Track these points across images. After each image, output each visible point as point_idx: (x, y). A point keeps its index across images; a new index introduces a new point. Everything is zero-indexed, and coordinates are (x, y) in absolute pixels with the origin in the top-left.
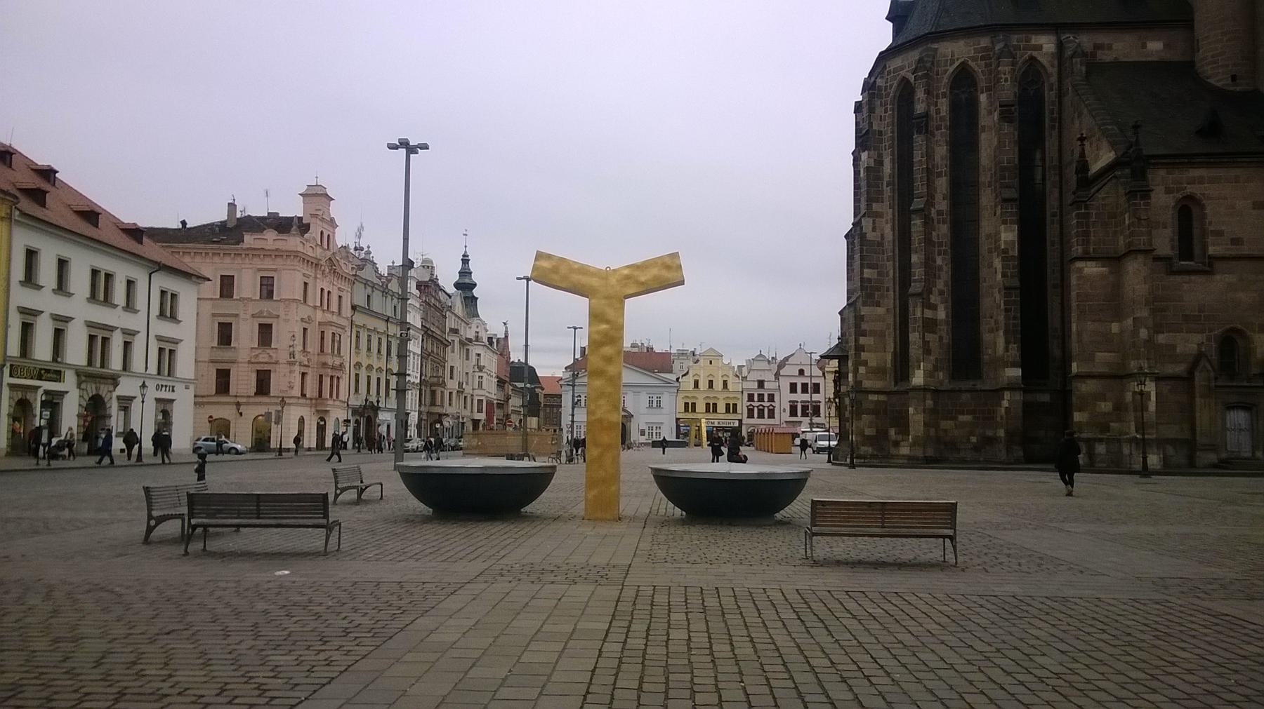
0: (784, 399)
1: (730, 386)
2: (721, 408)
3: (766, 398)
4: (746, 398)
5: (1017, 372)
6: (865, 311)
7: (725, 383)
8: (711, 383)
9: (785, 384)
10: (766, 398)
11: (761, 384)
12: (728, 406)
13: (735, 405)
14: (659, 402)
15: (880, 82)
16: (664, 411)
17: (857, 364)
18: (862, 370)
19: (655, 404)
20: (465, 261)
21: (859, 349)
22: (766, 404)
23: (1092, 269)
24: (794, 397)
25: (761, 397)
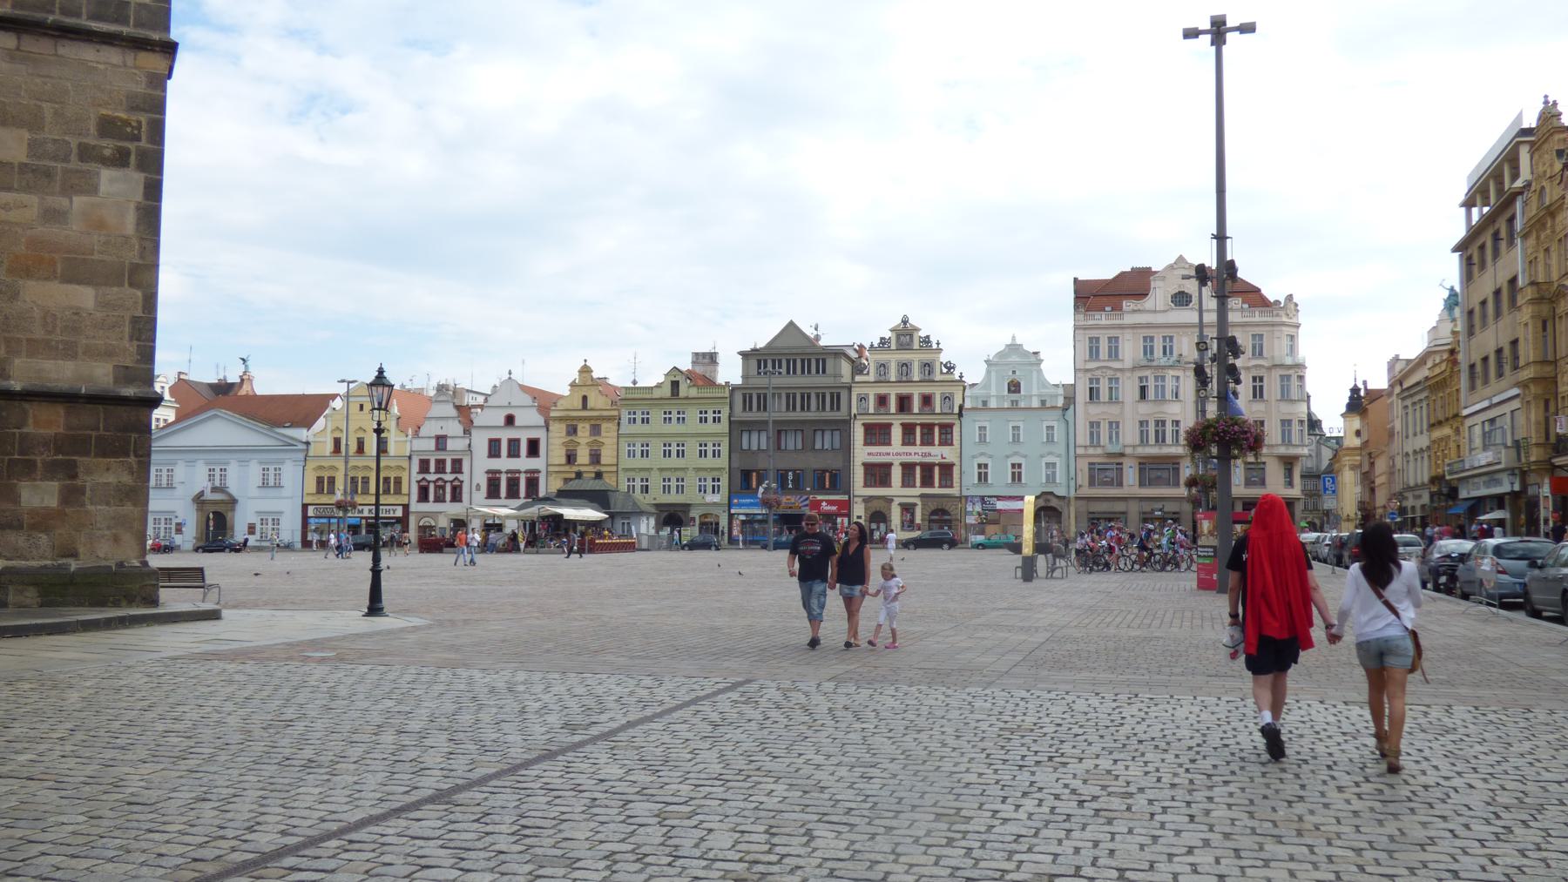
0: (479, 467)
3: (448, 468)
4: (415, 467)
9: (480, 442)
10: (448, 468)
11: (441, 441)
14: (278, 476)
16: (286, 492)
22: (449, 477)
24: (495, 464)
25: (440, 465)
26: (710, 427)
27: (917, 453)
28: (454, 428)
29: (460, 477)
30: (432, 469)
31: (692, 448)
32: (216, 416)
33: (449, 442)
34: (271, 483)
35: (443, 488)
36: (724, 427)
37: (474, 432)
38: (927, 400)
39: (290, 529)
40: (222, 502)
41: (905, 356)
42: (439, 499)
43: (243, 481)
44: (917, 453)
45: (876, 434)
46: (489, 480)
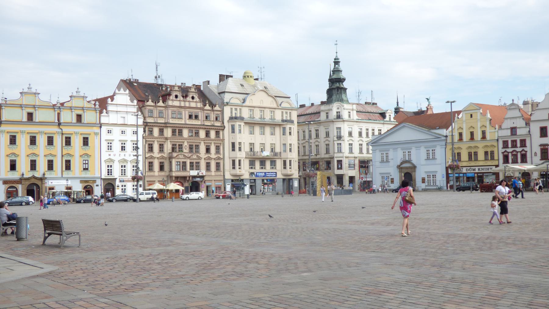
1: (488, 137)
2: (481, 156)
3: (519, 145)
4: (501, 145)
7: (484, 133)
8: (472, 134)
11: (513, 130)
12: (486, 153)
13: (492, 153)
14: (434, 154)
19: (431, 157)
20: (337, 62)
22: (519, 149)
25: (514, 143)
28: (520, 123)
29: (525, 149)
30: (510, 145)
32: (404, 126)
33: (518, 130)
34: (431, 157)
35: (516, 155)
37: (531, 124)
39: (441, 180)
40: (410, 168)
42: (515, 162)
43: (418, 157)
46: (542, 150)
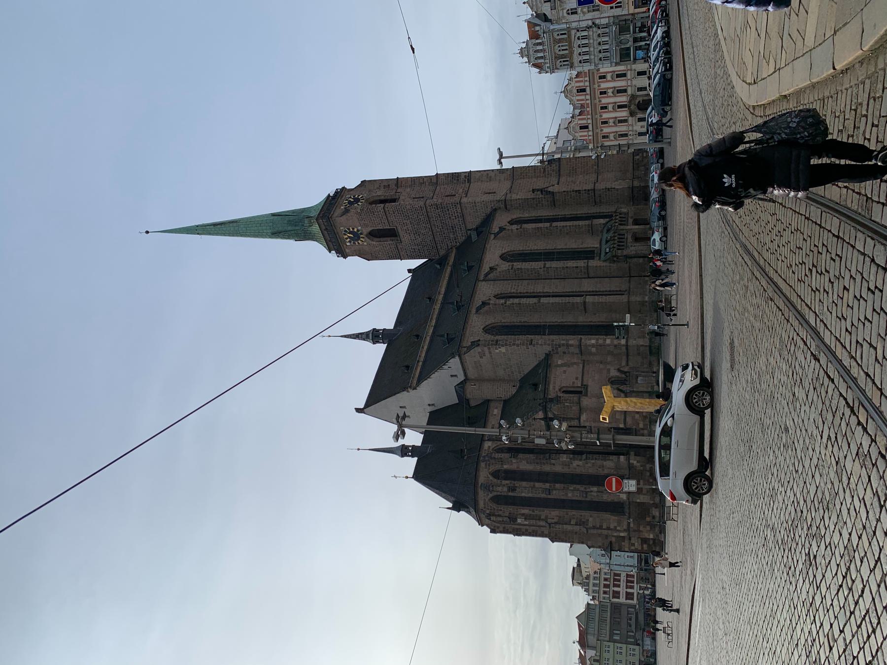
5: (622, 458)
6: (590, 525)
15: (488, 512)
17: (615, 529)
18: (618, 528)
21: (608, 528)
23: (584, 417)
26: (611, 649)
27: (623, 584)
31: (618, 657)
36: (611, 644)
38: (606, 580)
41: (591, 585)
44: (623, 584)
45: (616, 595)
